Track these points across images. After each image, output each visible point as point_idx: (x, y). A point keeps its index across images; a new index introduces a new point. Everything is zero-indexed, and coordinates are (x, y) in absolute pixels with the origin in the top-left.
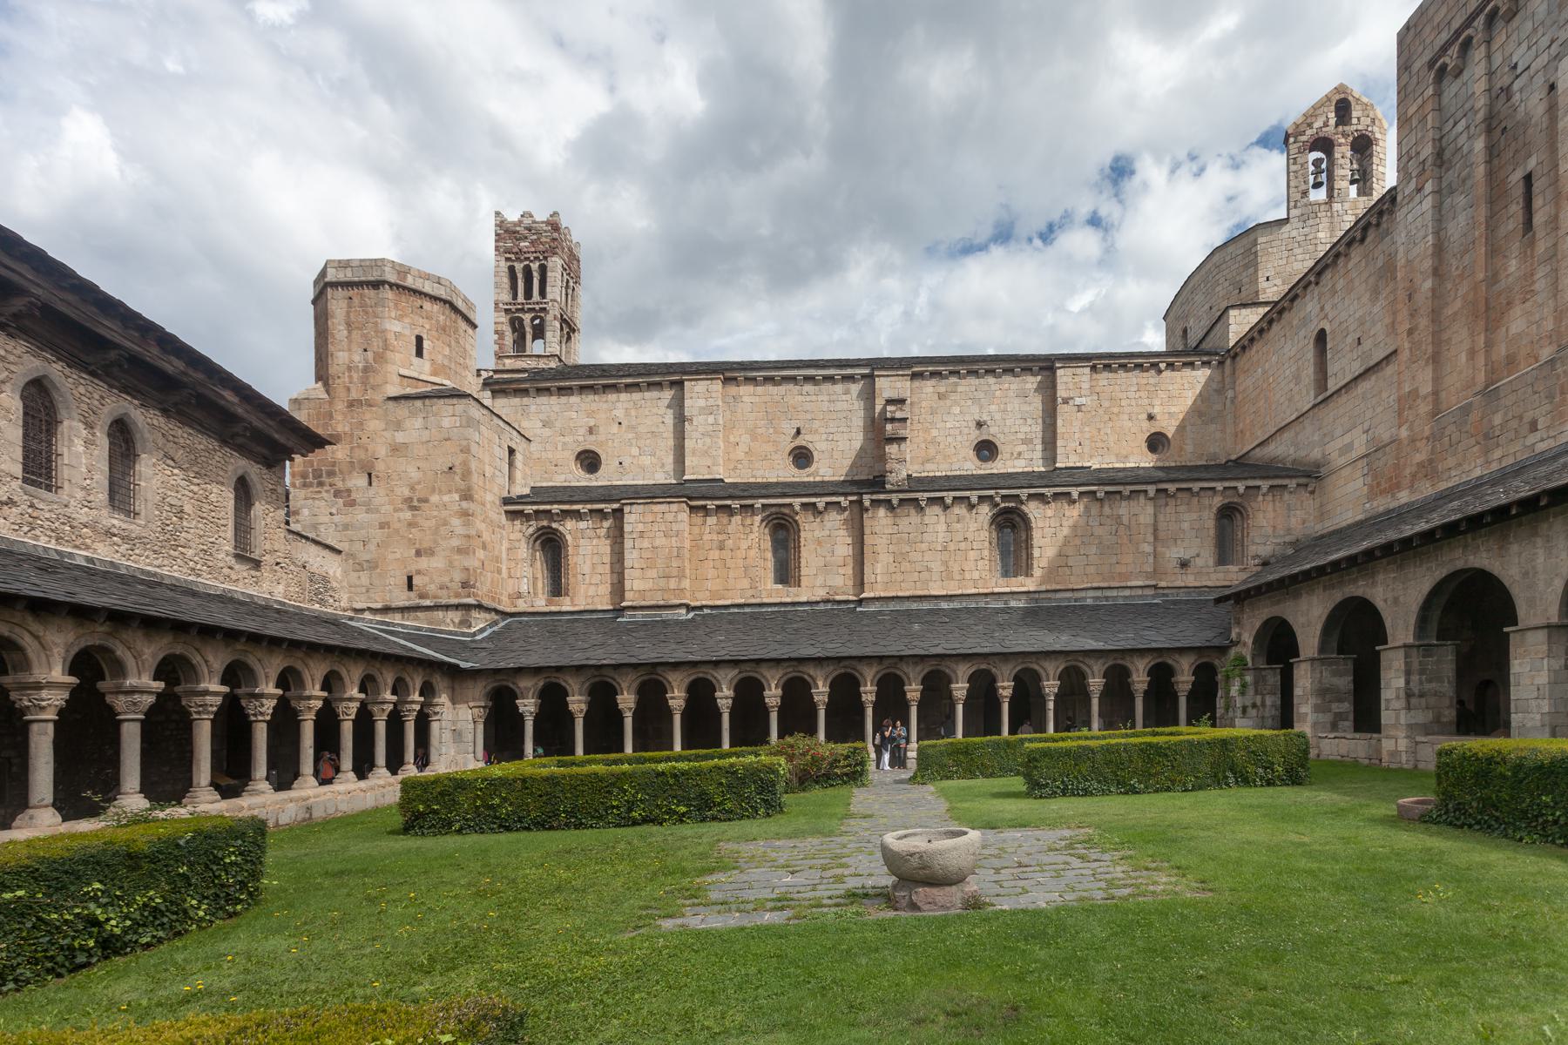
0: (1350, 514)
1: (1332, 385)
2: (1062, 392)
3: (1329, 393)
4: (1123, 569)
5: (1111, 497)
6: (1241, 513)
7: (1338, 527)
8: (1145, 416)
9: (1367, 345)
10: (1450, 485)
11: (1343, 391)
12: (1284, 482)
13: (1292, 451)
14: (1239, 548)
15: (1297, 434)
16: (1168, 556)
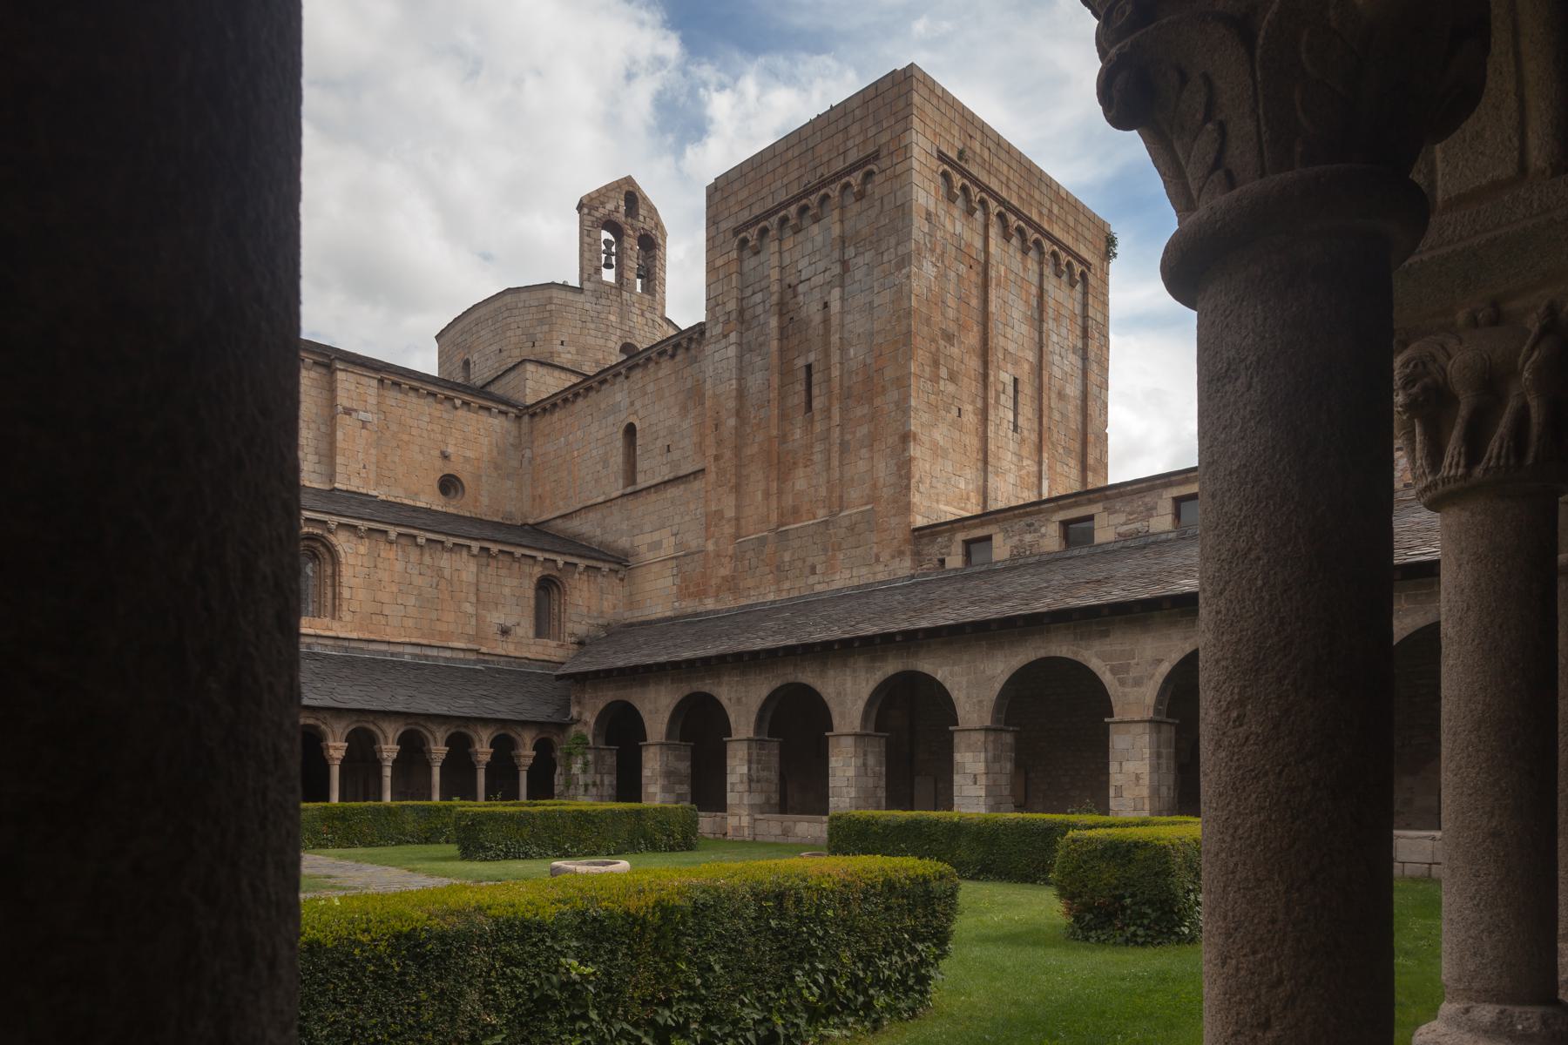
0: (659, 609)
1: (642, 481)
2: (343, 400)
3: (638, 487)
4: (444, 627)
5: (433, 545)
6: (558, 587)
7: (647, 618)
8: (437, 453)
9: (676, 455)
10: (750, 602)
11: (653, 490)
12: (600, 564)
13: (598, 532)
14: (556, 623)
15: (604, 518)
16: (488, 619)
